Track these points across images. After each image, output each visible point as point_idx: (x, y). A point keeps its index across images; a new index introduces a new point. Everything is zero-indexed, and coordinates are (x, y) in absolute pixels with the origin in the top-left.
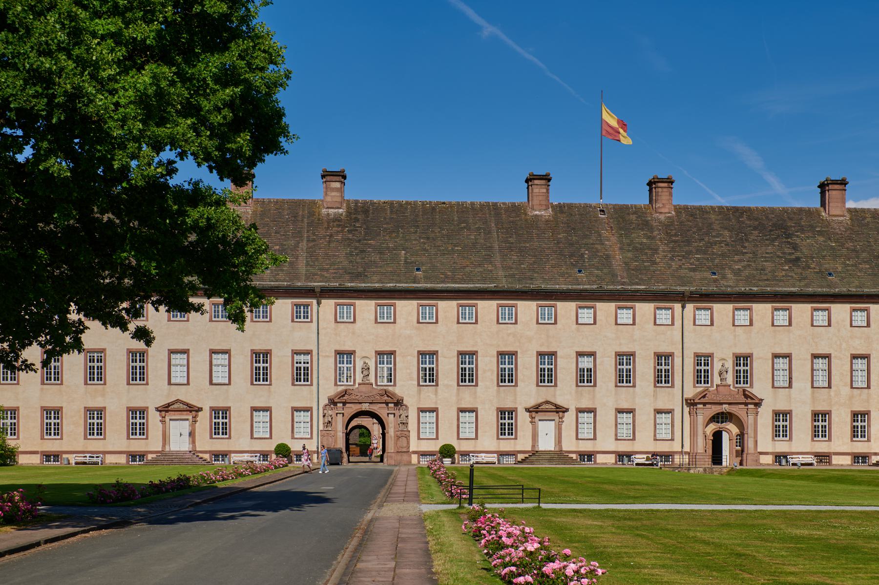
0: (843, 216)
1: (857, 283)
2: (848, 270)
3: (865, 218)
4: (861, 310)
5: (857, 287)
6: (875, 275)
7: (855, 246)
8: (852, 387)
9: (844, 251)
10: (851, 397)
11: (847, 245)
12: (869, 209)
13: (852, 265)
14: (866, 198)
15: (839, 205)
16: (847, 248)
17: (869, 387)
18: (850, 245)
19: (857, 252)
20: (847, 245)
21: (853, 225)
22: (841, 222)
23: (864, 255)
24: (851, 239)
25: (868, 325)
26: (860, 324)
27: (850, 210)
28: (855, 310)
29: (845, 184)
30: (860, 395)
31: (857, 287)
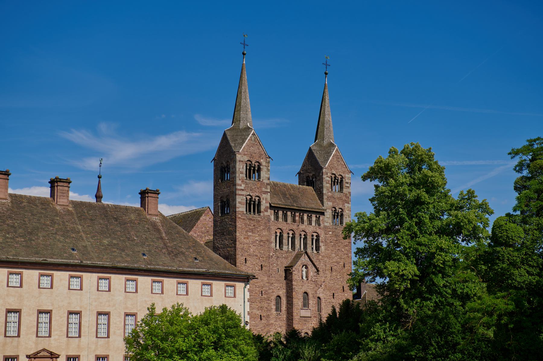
0: (6, 199)
1: (14, 252)
2: (7, 242)
3: (23, 202)
4: (17, 274)
5: (13, 255)
6: (28, 247)
7: (14, 224)
8: (5, 336)
9: (5, 227)
10: (5, 344)
11: (7, 222)
12: (25, 196)
13: (11, 238)
14: (21, 187)
15: (3, 190)
16: (8, 225)
17: (19, 336)
18: (10, 222)
19: (15, 228)
20: (7, 222)
21: (13, 207)
22: (4, 204)
23: (21, 230)
24: (11, 218)
25: (21, 286)
26: (14, 285)
27: (11, 195)
28: (11, 273)
29: (8, 175)
30: (12, 342)
31: (13, 255)
